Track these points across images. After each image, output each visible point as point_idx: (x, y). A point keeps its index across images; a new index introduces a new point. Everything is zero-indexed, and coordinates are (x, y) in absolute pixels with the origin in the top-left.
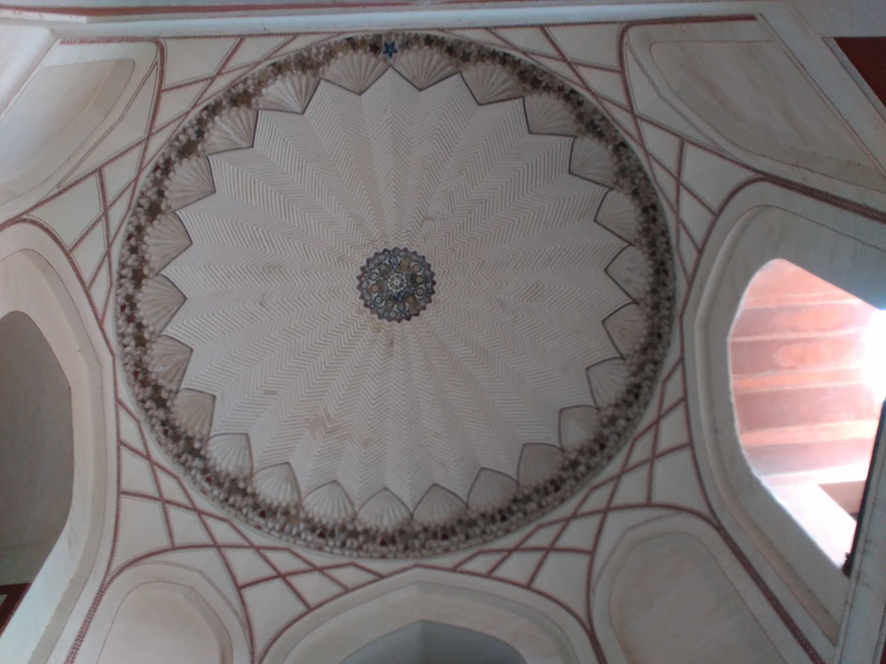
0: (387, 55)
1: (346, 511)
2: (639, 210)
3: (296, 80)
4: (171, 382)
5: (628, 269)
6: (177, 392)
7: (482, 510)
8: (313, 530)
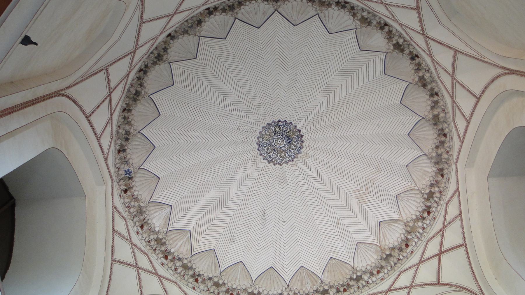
0: (131, 174)
1: (417, 194)
2: (212, 16)
3: (152, 212)
4: (317, 282)
5: (256, 14)
6: (322, 282)
7: (429, 108)
8: (423, 218)
